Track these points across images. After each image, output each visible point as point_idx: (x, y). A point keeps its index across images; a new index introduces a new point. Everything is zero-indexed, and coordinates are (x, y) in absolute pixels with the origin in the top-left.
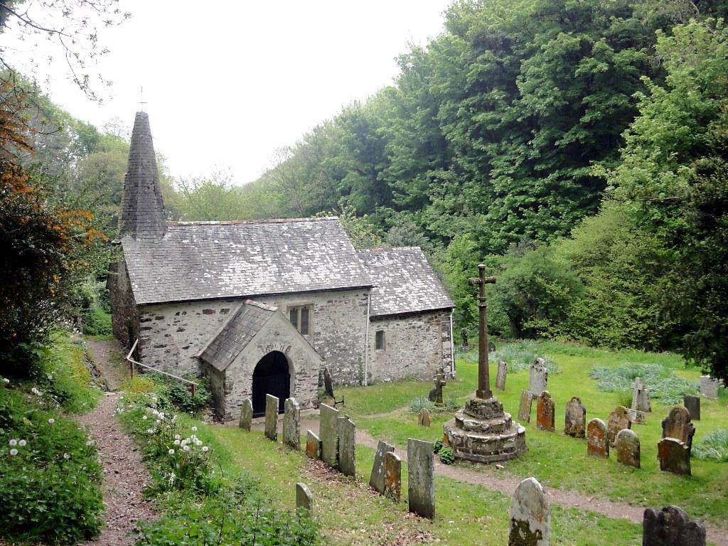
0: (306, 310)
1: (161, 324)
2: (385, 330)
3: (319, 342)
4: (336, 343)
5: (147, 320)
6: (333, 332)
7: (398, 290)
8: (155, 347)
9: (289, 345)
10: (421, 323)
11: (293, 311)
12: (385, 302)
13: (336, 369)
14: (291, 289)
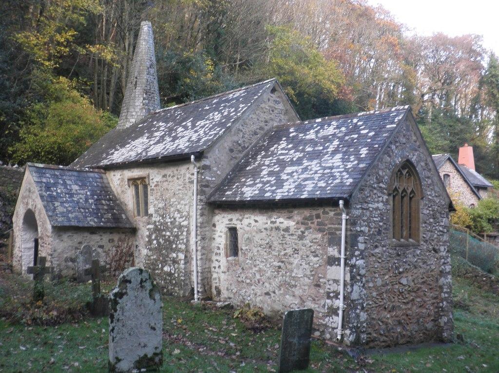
10: (291, 224)
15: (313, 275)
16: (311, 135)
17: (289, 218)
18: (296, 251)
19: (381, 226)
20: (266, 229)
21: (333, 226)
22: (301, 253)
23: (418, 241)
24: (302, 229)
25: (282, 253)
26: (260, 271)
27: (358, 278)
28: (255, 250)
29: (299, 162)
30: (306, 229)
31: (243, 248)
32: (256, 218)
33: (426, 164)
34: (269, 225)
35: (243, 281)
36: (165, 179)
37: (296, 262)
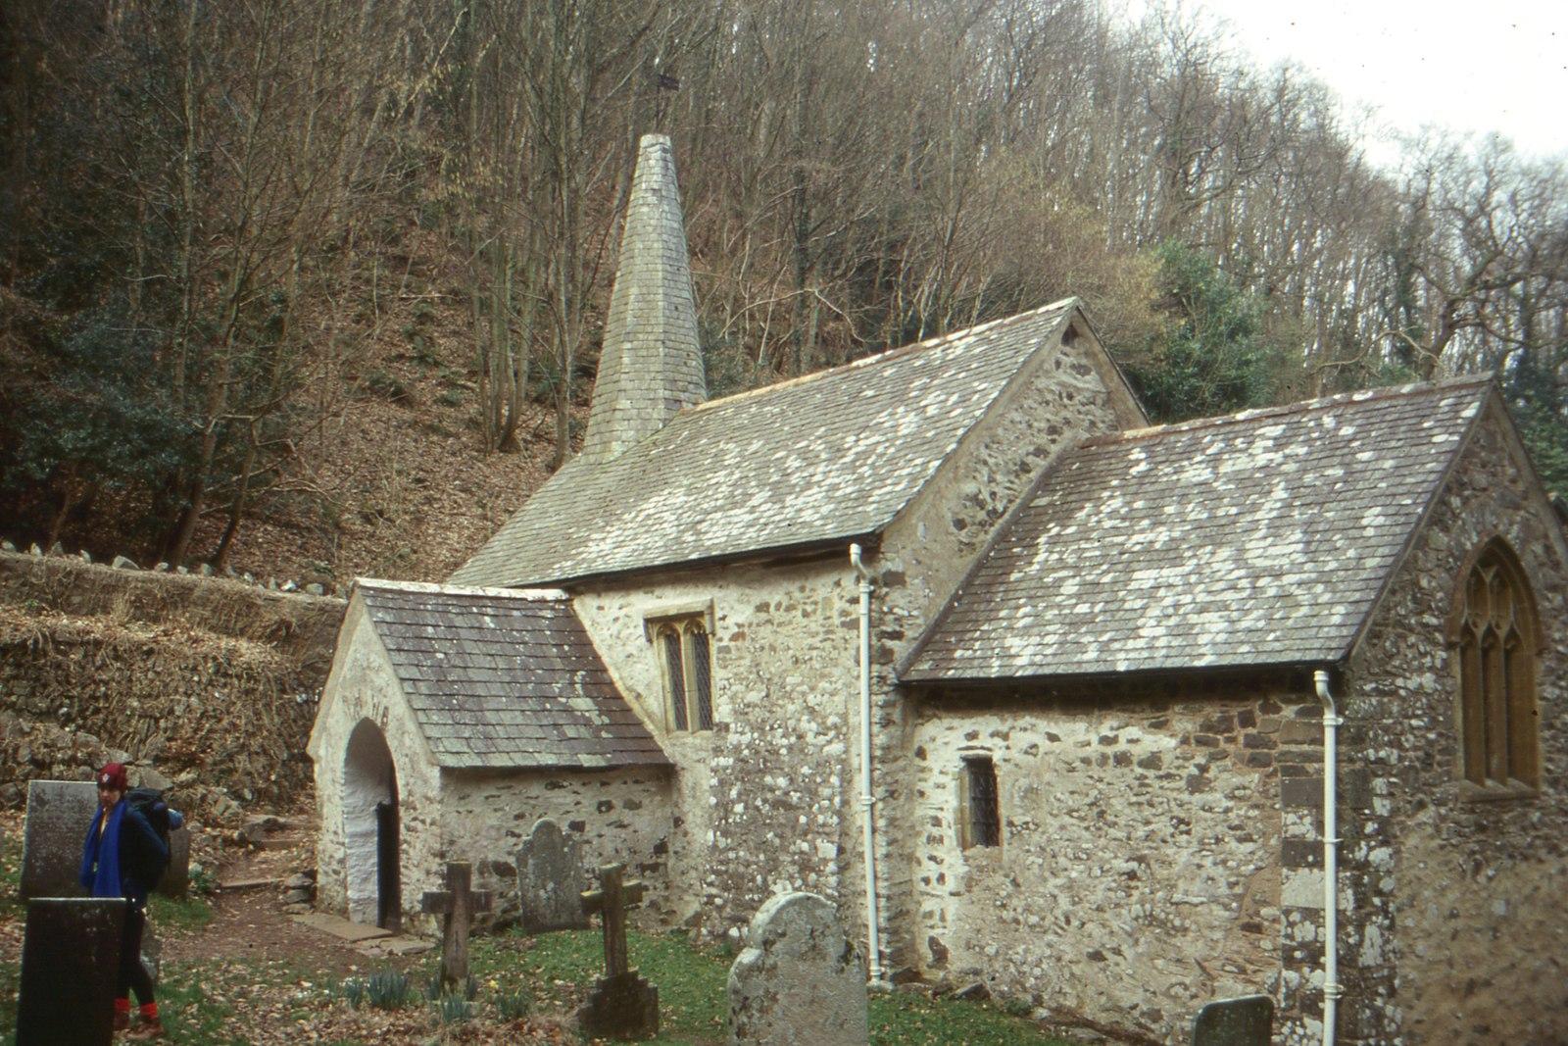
4: (763, 772)
10: (1164, 743)
13: (753, 880)
15: (1239, 898)
16: (1195, 472)
17: (1159, 726)
19: (1431, 743)
20: (1086, 761)
21: (1294, 748)
23: (1533, 783)
24: (1201, 760)
25: (1141, 831)
26: (1070, 886)
27: (1377, 901)
28: (1053, 824)
29: (1171, 555)
30: (1213, 758)
31: (1018, 820)
32: (1054, 730)
33: (1548, 549)
34: (1095, 749)
35: (1017, 921)
36: (763, 616)
37: (1183, 857)
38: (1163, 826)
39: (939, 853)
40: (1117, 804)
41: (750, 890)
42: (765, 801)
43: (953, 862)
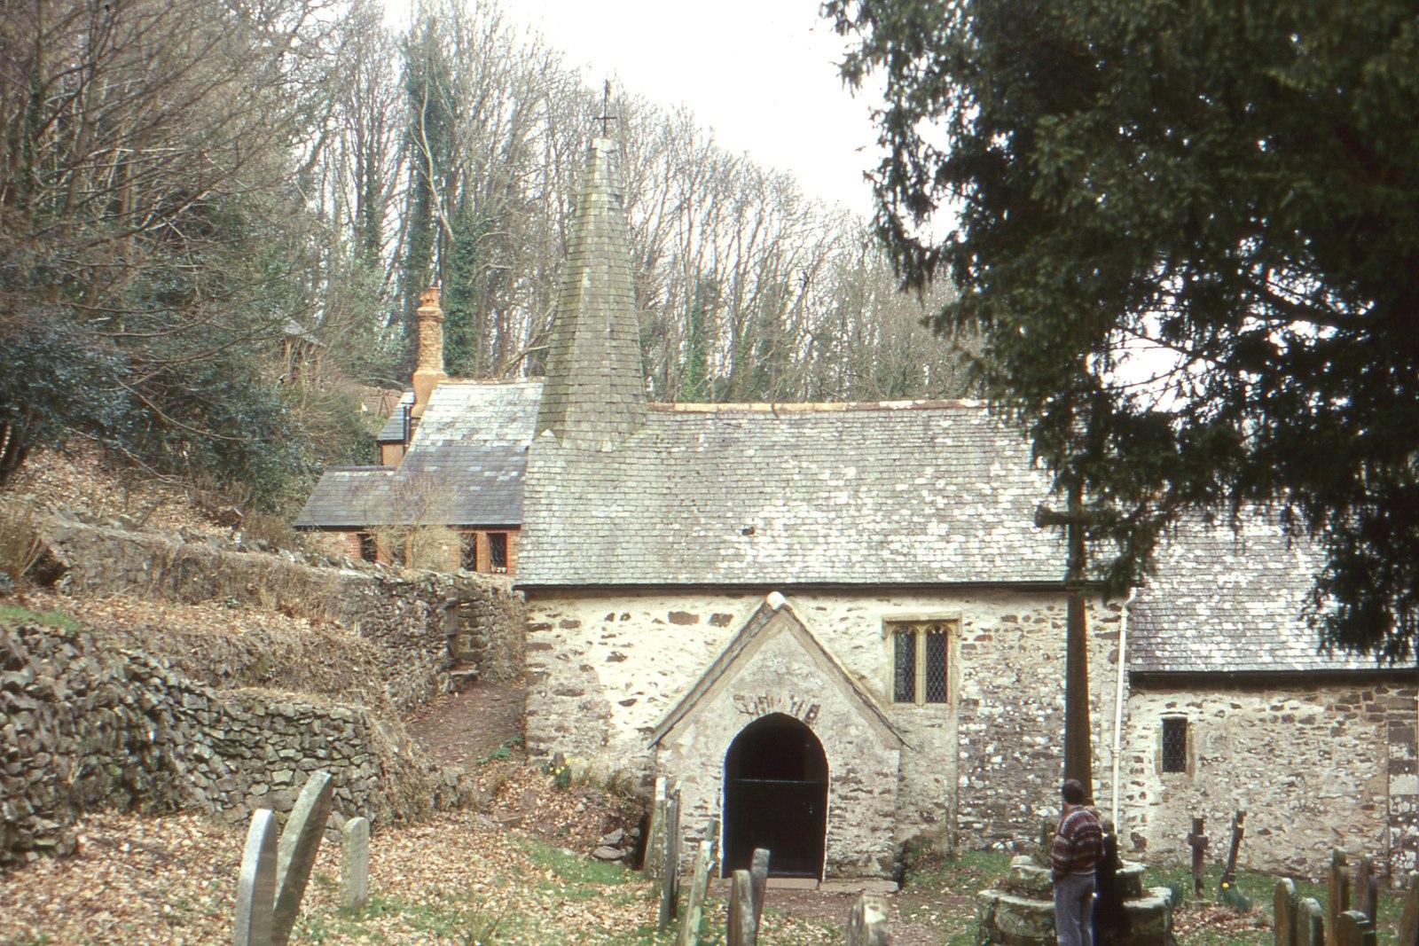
0: (939, 634)
1: (573, 640)
2: (1192, 716)
3: (973, 727)
4: (1021, 734)
5: (542, 627)
6: (1014, 702)
7: (1257, 608)
8: (558, 693)
9: (815, 701)
10: (1316, 709)
11: (903, 631)
12: (1200, 637)
13: (1016, 807)
14: (899, 577)
15: (1361, 792)
17: (1310, 700)
18: (1326, 754)
20: (1262, 720)
21: (1395, 712)
22: (1336, 757)
24: (1340, 719)
25: (1299, 759)
26: (1248, 794)
28: (1236, 758)
30: (1347, 717)
32: (1236, 701)
34: (1268, 714)
36: (1010, 625)
37: (1326, 772)
38: (1314, 756)
39: (1140, 779)
40: (1283, 744)
41: (1014, 815)
42: (1023, 754)
43: (1153, 783)
